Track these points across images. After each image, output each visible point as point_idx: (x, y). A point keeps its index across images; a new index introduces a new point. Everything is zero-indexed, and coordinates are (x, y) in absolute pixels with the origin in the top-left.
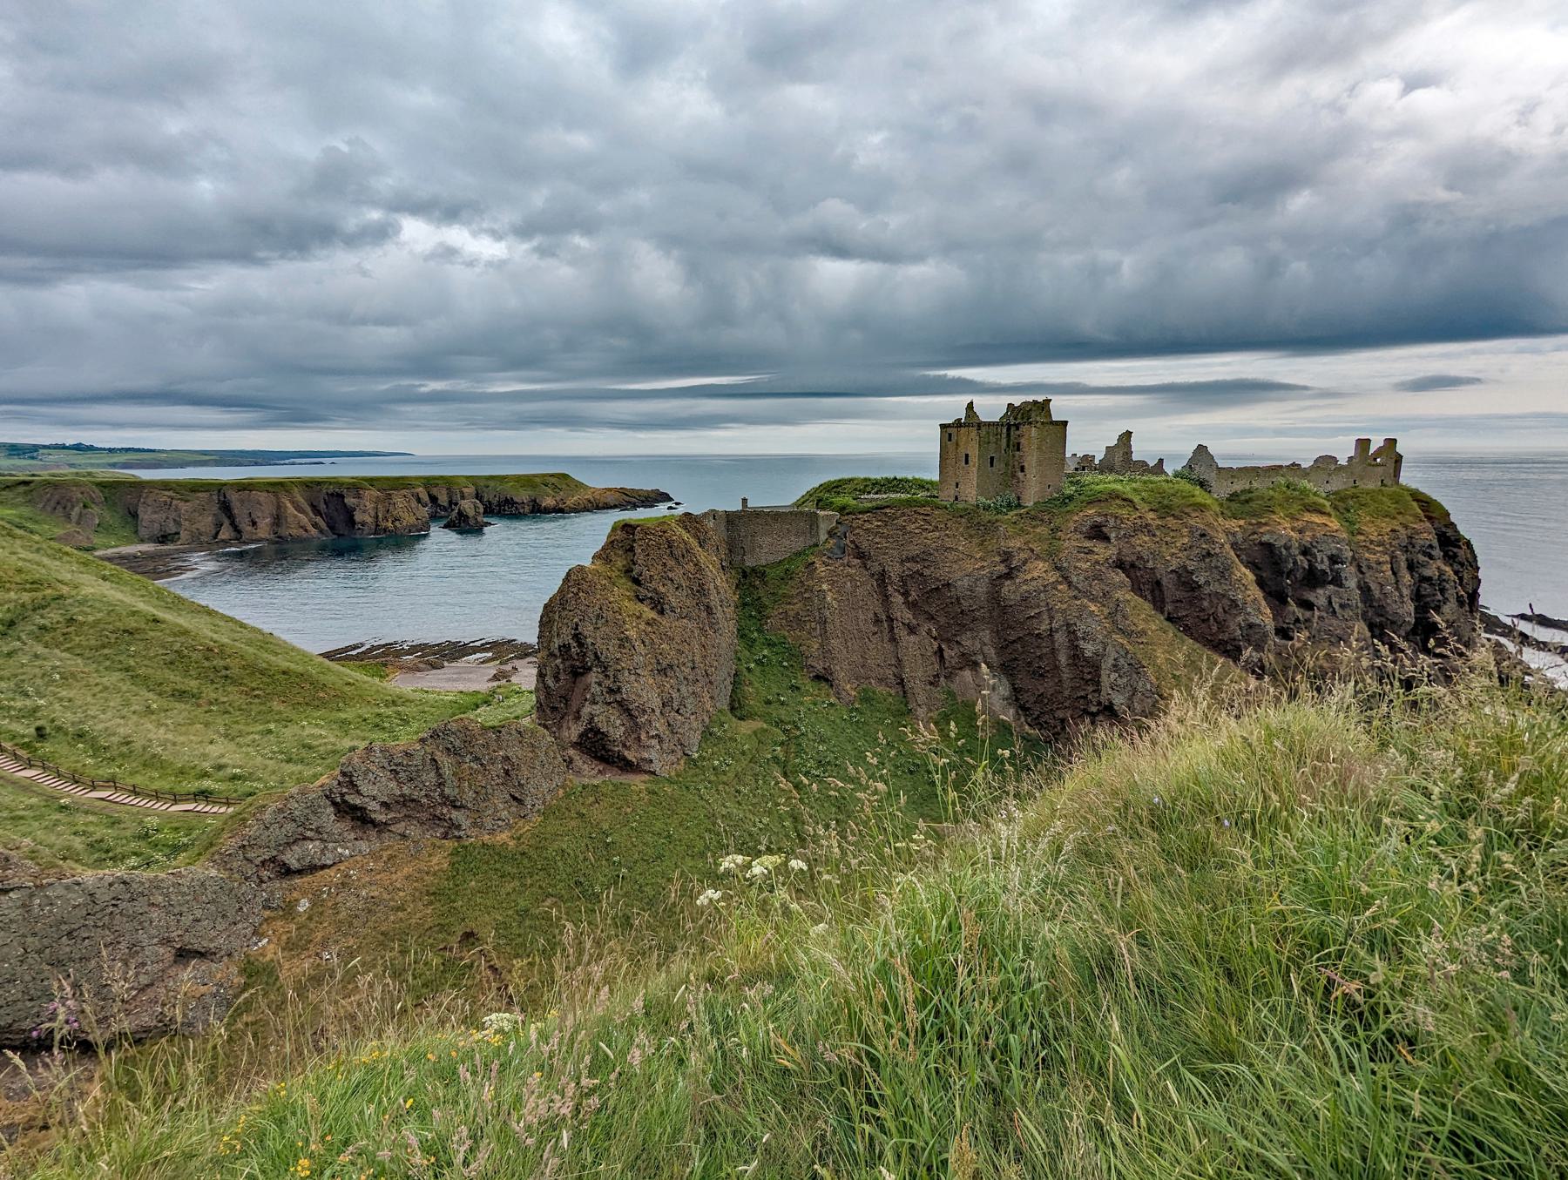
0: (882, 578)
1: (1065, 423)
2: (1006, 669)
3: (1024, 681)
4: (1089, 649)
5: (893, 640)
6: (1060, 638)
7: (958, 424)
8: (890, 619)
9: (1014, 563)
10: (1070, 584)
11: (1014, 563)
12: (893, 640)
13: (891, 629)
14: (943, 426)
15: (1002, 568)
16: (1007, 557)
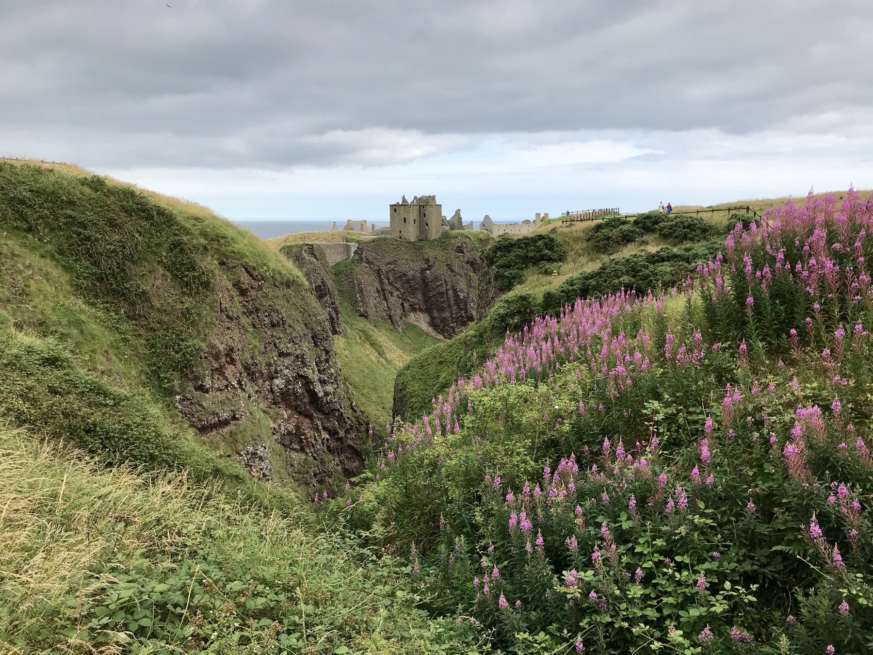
0: (379, 272)
1: (441, 206)
2: (428, 311)
3: (436, 314)
4: (461, 295)
5: (386, 299)
6: (451, 292)
7: (397, 205)
8: (383, 290)
9: (431, 263)
10: (452, 271)
11: (431, 263)
12: (386, 299)
13: (384, 295)
14: (391, 206)
15: (426, 266)
16: (427, 261)
